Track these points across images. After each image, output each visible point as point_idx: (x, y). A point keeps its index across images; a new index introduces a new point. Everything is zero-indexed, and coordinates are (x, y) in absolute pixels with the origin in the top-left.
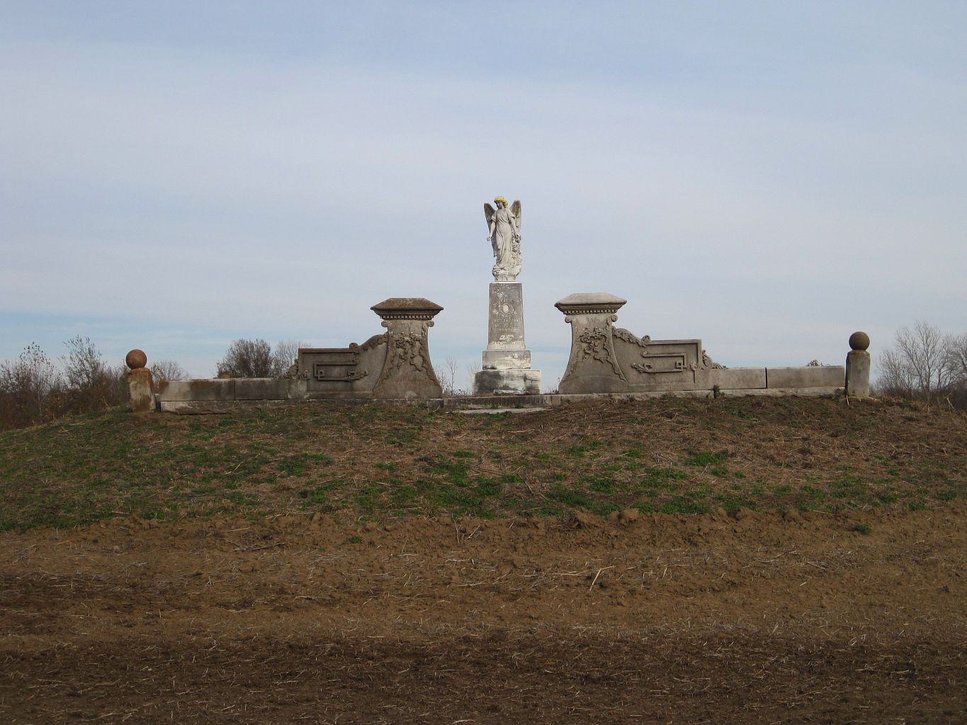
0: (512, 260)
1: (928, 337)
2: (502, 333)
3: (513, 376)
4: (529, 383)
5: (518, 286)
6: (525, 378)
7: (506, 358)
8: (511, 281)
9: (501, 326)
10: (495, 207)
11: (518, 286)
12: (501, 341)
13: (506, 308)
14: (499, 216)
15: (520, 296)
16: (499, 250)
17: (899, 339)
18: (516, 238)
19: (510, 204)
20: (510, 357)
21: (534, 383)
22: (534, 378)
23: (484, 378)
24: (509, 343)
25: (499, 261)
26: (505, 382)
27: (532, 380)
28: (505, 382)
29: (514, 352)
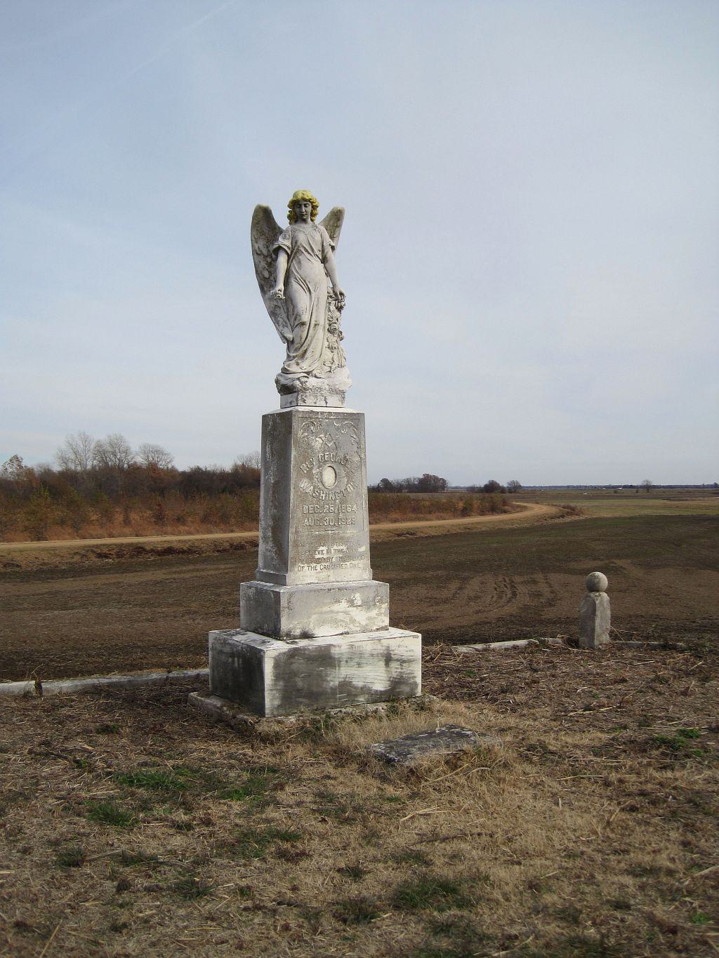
0: (328, 355)
1: (86, 440)
2: (321, 540)
3: (361, 655)
4: (395, 668)
5: (356, 420)
6: (388, 659)
7: (336, 607)
8: (334, 406)
9: (319, 523)
10: (281, 218)
12: (318, 561)
13: (328, 476)
14: (302, 238)
15: (360, 446)
16: (303, 324)
17: (68, 442)
18: (337, 298)
19: (323, 213)
20: (343, 605)
21: (407, 669)
22: (406, 655)
23: (294, 667)
24: (334, 566)
25: (296, 348)
27: (402, 662)
29: (354, 590)
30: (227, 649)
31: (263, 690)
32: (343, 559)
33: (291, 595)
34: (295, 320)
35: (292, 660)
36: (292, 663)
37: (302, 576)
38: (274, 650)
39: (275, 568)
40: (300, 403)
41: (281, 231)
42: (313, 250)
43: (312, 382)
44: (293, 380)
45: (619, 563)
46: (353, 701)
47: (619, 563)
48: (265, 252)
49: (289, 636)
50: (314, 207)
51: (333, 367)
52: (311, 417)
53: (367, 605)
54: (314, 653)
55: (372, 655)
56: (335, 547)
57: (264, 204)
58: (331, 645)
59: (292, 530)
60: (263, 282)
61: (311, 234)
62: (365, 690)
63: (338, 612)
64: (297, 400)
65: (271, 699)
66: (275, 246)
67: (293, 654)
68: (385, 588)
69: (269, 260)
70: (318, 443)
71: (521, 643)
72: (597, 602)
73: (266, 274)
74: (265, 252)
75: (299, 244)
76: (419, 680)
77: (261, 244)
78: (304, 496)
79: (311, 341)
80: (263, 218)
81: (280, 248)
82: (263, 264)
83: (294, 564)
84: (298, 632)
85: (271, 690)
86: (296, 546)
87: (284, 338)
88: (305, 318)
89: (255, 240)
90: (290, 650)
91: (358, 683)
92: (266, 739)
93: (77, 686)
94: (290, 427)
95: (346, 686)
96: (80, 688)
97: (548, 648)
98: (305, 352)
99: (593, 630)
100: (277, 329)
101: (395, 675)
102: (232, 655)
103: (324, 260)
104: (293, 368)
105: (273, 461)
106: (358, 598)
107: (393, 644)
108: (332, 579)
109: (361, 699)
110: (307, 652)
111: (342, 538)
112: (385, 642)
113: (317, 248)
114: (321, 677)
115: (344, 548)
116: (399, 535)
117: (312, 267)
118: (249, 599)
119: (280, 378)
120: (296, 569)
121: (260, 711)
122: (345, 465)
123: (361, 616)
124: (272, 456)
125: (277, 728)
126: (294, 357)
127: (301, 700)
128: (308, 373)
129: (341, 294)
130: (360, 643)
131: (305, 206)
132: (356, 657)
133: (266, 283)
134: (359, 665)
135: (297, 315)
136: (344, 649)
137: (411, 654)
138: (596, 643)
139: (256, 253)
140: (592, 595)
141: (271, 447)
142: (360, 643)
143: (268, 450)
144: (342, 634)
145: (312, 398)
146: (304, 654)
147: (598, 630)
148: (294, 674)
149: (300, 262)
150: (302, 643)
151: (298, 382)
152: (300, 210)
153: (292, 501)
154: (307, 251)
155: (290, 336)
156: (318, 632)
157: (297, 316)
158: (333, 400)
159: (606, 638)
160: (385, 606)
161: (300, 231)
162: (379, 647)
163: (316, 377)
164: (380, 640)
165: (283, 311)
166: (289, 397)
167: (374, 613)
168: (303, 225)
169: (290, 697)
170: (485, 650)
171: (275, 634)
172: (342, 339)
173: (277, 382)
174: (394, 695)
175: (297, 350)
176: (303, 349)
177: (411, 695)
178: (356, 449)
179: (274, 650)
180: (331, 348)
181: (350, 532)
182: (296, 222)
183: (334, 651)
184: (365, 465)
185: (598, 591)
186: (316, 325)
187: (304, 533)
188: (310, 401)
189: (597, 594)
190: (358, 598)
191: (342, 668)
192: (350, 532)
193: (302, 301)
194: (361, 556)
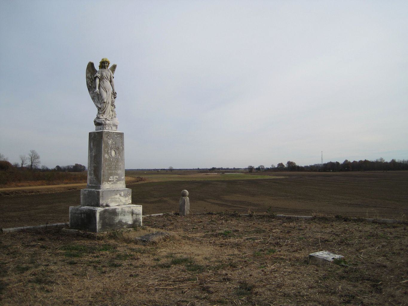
2: (111, 174)
5: (121, 135)
6: (133, 213)
7: (116, 196)
8: (114, 130)
9: (110, 168)
10: (97, 67)
11: (121, 135)
12: (110, 181)
13: (113, 153)
14: (104, 74)
16: (105, 102)
18: (114, 94)
19: (111, 65)
20: (118, 196)
22: (138, 212)
23: (105, 215)
24: (115, 183)
25: (102, 111)
26: (120, 217)
27: (137, 214)
28: (120, 217)
29: (121, 191)
30: (79, 212)
31: (96, 223)
32: (117, 181)
33: (103, 192)
34: (102, 101)
35: (105, 213)
36: (104, 214)
37: (106, 186)
38: (99, 210)
39: (95, 184)
40: (104, 129)
41: (96, 71)
42: (108, 78)
43: (107, 122)
44: (102, 121)
45: (165, 199)
46: (123, 227)
47: (165, 199)
48: (90, 77)
49: (102, 206)
50: (109, 64)
51: (113, 117)
52: (108, 133)
53: (125, 196)
54: (111, 211)
55: (128, 212)
56: (115, 177)
57: (92, 61)
58: (116, 209)
59: (102, 171)
60: (89, 88)
61: (107, 73)
62: (126, 224)
63: (116, 198)
64: (103, 128)
65: (98, 226)
66: (95, 76)
67: (105, 211)
68: (130, 190)
69: (91, 80)
70: (110, 142)
71: (161, 214)
72: (185, 200)
73: (90, 85)
74: (90, 77)
75: (103, 76)
76: (141, 221)
77: (89, 75)
78: (106, 160)
79: (107, 108)
80: (91, 66)
81: (97, 77)
82: (89, 81)
83: (103, 183)
84: (105, 204)
85: (99, 223)
86: (103, 176)
87: (97, 106)
88: (105, 101)
89: (87, 73)
90: (104, 210)
91: (124, 221)
92: (99, 239)
93: (15, 229)
94: (102, 136)
95: (120, 222)
96: (16, 230)
97: (170, 216)
98: (105, 112)
99: (184, 210)
100: (95, 104)
101: (134, 219)
102: (81, 214)
103: (111, 82)
104: (101, 117)
105: (94, 148)
106: (122, 193)
107: (134, 208)
108: (114, 187)
109: (125, 227)
110: (109, 211)
111: (117, 174)
112: (132, 208)
113: (109, 77)
114: (113, 219)
115: (117, 177)
116: (69, 189)
117: (107, 84)
118: (85, 195)
119: (96, 120)
120: (103, 184)
121: (94, 230)
122: (118, 150)
123: (123, 200)
124: (94, 146)
125: (102, 235)
126: (101, 113)
127: (107, 227)
128: (106, 119)
129: (116, 93)
130: (124, 208)
131: (106, 63)
132: (123, 213)
133: (91, 87)
134: (124, 215)
135: (102, 99)
136: (120, 210)
137: (139, 212)
138: (185, 214)
139: (87, 77)
140: (183, 198)
141: (93, 143)
142: (124, 208)
143: (92, 144)
144: (118, 205)
145: (108, 127)
146: (108, 211)
147: (186, 209)
148: (105, 218)
149: (103, 82)
150: (107, 208)
151: (103, 122)
152: (104, 64)
153: (102, 161)
154: (106, 79)
155: (100, 106)
156: (111, 205)
157: (103, 100)
158: (114, 128)
159: (188, 213)
160: (130, 196)
161: (104, 72)
162: (130, 209)
163: (108, 120)
164: (130, 207)
165: (97, 98)
166: (100, 127)
167: (127, 198)
168: (105, 70)
169: (104, 225)
170: (150, 216)
171: (98, 205)
172: (115, 108)
173: (95, 121)
174: (134, 226)
175: (102, 111)
176: (104, 111)
177: (140, 226)
178: (121, 144)
179: (99, 210)
180: (112, 111)
181: (119, 172)
182: (102, 68)
183: (117, 210)
184: (124, 149)
185: (185, 196)
186: (108, 103)
187: (106, 172)
188: (107, 128)
189: (185, 197)
190: (122, 193)
191: (119, 216)
192: (119, 172)
193: (104, 95)
194: (122, 180)
